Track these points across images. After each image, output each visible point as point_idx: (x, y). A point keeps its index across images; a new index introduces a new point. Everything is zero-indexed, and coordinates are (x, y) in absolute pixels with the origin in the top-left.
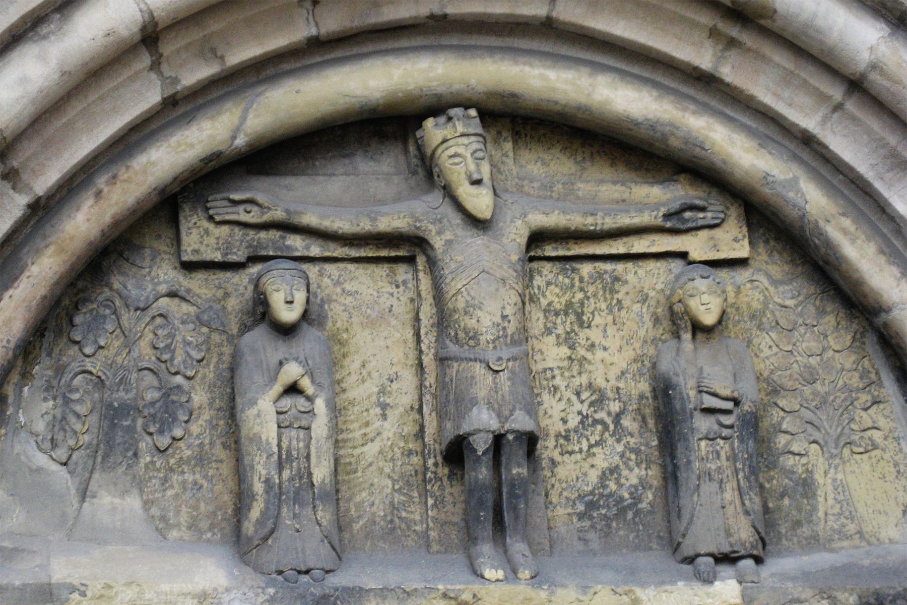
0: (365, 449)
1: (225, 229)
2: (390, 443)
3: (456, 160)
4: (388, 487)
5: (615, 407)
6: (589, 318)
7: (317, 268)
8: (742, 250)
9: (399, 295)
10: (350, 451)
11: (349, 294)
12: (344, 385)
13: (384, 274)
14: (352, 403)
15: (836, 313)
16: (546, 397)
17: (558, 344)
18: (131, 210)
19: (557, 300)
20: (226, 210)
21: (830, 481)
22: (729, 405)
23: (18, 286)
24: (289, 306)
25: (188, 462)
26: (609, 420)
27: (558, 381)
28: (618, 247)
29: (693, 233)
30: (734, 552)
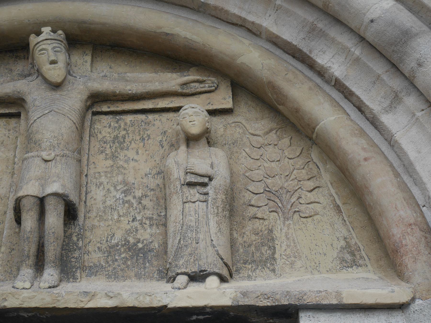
3: (42, 52)
5: (139, 194)
6: (128, 144)
8: (228, 104)
9: (9, 135)
15: (290, 137)
16: (93, 188)
17: (106, 159)
19: (108, 135)
21: (284, 234)
22: (206, 180)
26: (134, 201)
27: (103, 179)
28: (148, 105)
29: (197, 96)
30: (201, 271)
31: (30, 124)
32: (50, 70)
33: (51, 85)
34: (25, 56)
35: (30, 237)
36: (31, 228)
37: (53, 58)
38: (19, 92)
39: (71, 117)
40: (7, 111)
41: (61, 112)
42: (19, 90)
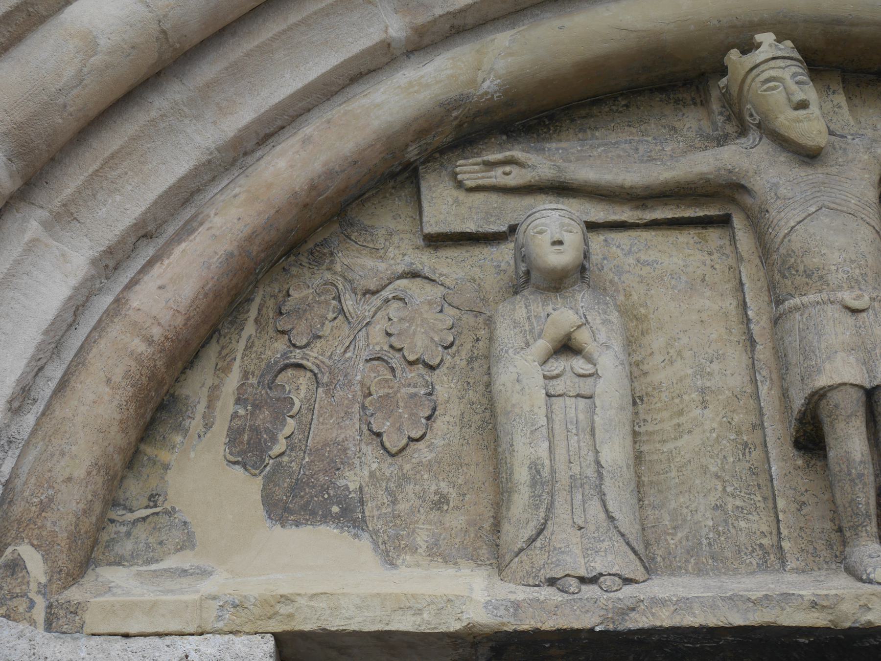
0: (679, 443)
1: (479, 198)
2: (714, 435)
3: (772, 84)
4: (716, 489)
7: (602, 238)
9: (712, 263)
10: (658, 446)
11: (647, 263)
12: (645, 367)
13: (692, 241)
14: (658, 388)
18: (350, 160)
20: (479, 175)
23: (195, 239)
24: (557, 247)
25: (429, 466)
31: (781, 235)
32: (798, 120)
33: (800, 154)
34: (693, 99)
35: (863, 475)
36: (863, 455)
37: (799, 96)
38: (730, 172)
39: (868, 220)
40: (700, 213)
41: (845, 209)
42: (730, 167)
